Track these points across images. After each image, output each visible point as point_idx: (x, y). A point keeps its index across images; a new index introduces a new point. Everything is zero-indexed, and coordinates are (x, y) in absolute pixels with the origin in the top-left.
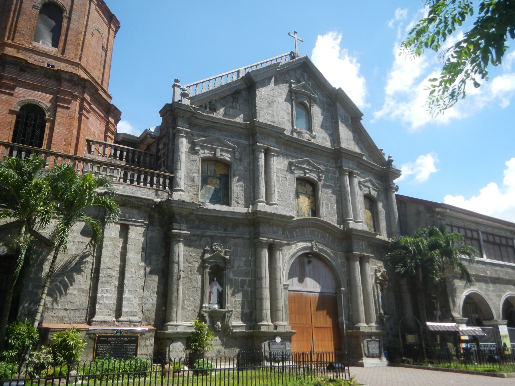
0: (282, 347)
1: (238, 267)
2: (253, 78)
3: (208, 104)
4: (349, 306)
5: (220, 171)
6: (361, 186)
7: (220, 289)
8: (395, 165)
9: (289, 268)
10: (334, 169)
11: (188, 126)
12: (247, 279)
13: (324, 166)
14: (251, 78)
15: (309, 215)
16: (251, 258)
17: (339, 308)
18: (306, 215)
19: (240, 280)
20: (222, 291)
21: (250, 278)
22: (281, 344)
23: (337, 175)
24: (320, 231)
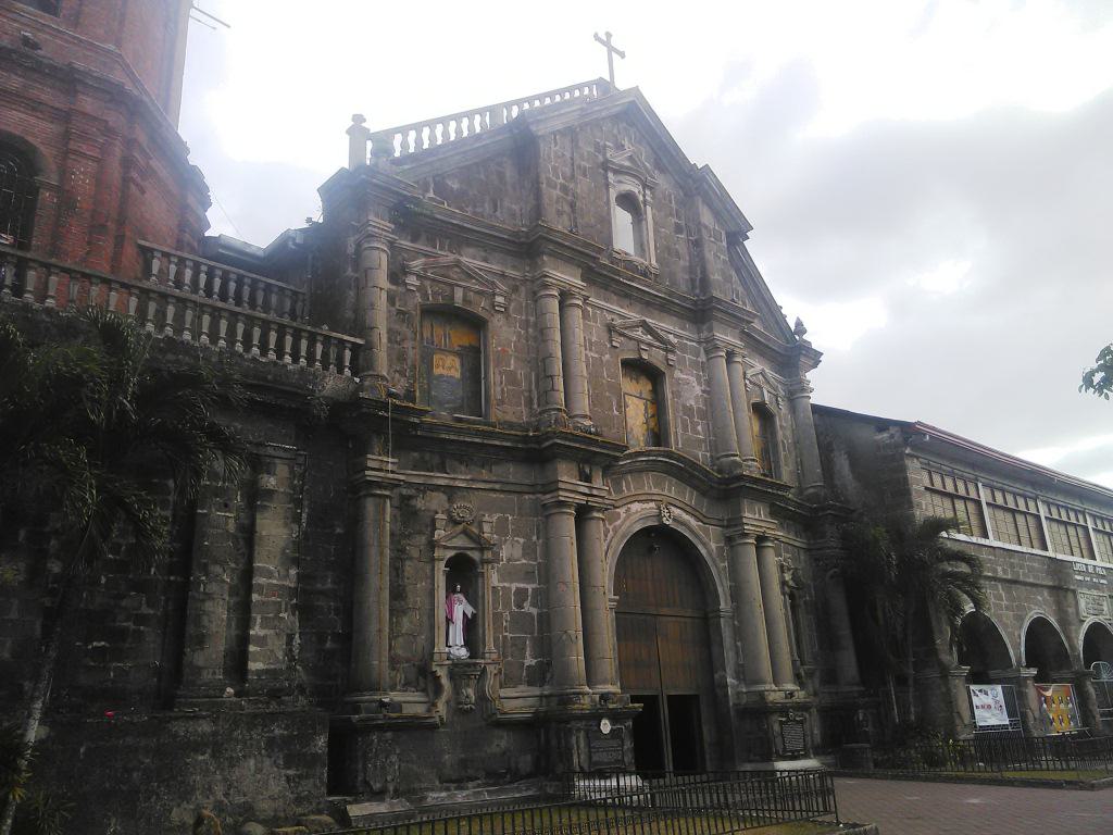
0: (614, 743)
1: (509, 560)
3: (431, 180)
4: (736, 646)
5: (459, 337)
6: (747, 382)
7: (470, 610)
8: (815, 338)
11: (393, 226)
12: (530, 587)
13: (676, 336)
15: (647, 444)
16: (538, 538)
17: (715, 649)
18: (642, 444)
19: (514, 589)
20: (474, 615)
21: (534, 586)
23: (703, 358)
24: (675, 480)
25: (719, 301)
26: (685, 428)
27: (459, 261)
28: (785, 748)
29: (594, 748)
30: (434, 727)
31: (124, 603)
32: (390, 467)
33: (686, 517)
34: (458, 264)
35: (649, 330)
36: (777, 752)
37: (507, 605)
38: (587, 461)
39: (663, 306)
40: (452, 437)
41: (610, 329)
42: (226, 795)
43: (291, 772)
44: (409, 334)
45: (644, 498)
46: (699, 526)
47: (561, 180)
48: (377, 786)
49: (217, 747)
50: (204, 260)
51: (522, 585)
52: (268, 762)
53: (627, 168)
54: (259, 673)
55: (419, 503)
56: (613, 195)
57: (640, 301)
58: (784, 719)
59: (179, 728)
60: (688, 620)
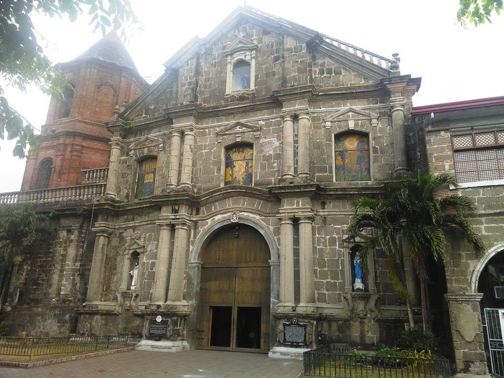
0: (163, 326)
1: (150, 251)
2: (172, 67)
9: (201, 244)
10: (278, 119)
13: (263, 120)
14: (171, 68)
15: (245, 183)
19: (150, 262)
22: (162, 324)
24: (247, 198)
25: (277, 92)
26: (263, 168)
27: (147, 137)
28: (285, 339)
29: (152, 327)
30: (116, 314)
31: (41, 276)
32: (102, 225)
33: (251, 215)
34: (147, 138)
35: (243, 125)
36: (279, 341)
37: (147, 269)
38: (175, 204)
39: (254, 109)
40: (131, 208)
41: (218, 134)
42: (43, 329)
43: (59, 325)
44: (130, 172)
45: (224, 211)
46: (260, 219)
47: (189, 80)
48: (81, 332)
49: (42, 315)
50: (86, 170)
51: (153, 261)
52: (53, 321)
53: (241, 47)
54: (63, 295)
55: (124, 235)
56: (230, 67)
57: (240, 112)
58: (287, 323)
59: (35, 310)
60: (260, 268)
